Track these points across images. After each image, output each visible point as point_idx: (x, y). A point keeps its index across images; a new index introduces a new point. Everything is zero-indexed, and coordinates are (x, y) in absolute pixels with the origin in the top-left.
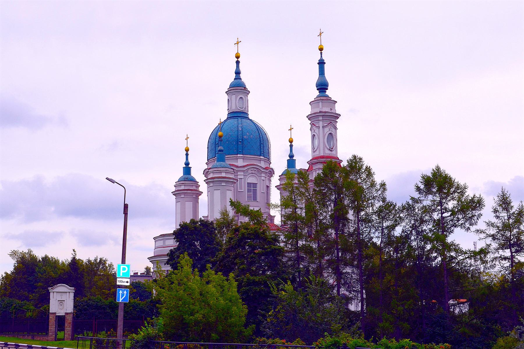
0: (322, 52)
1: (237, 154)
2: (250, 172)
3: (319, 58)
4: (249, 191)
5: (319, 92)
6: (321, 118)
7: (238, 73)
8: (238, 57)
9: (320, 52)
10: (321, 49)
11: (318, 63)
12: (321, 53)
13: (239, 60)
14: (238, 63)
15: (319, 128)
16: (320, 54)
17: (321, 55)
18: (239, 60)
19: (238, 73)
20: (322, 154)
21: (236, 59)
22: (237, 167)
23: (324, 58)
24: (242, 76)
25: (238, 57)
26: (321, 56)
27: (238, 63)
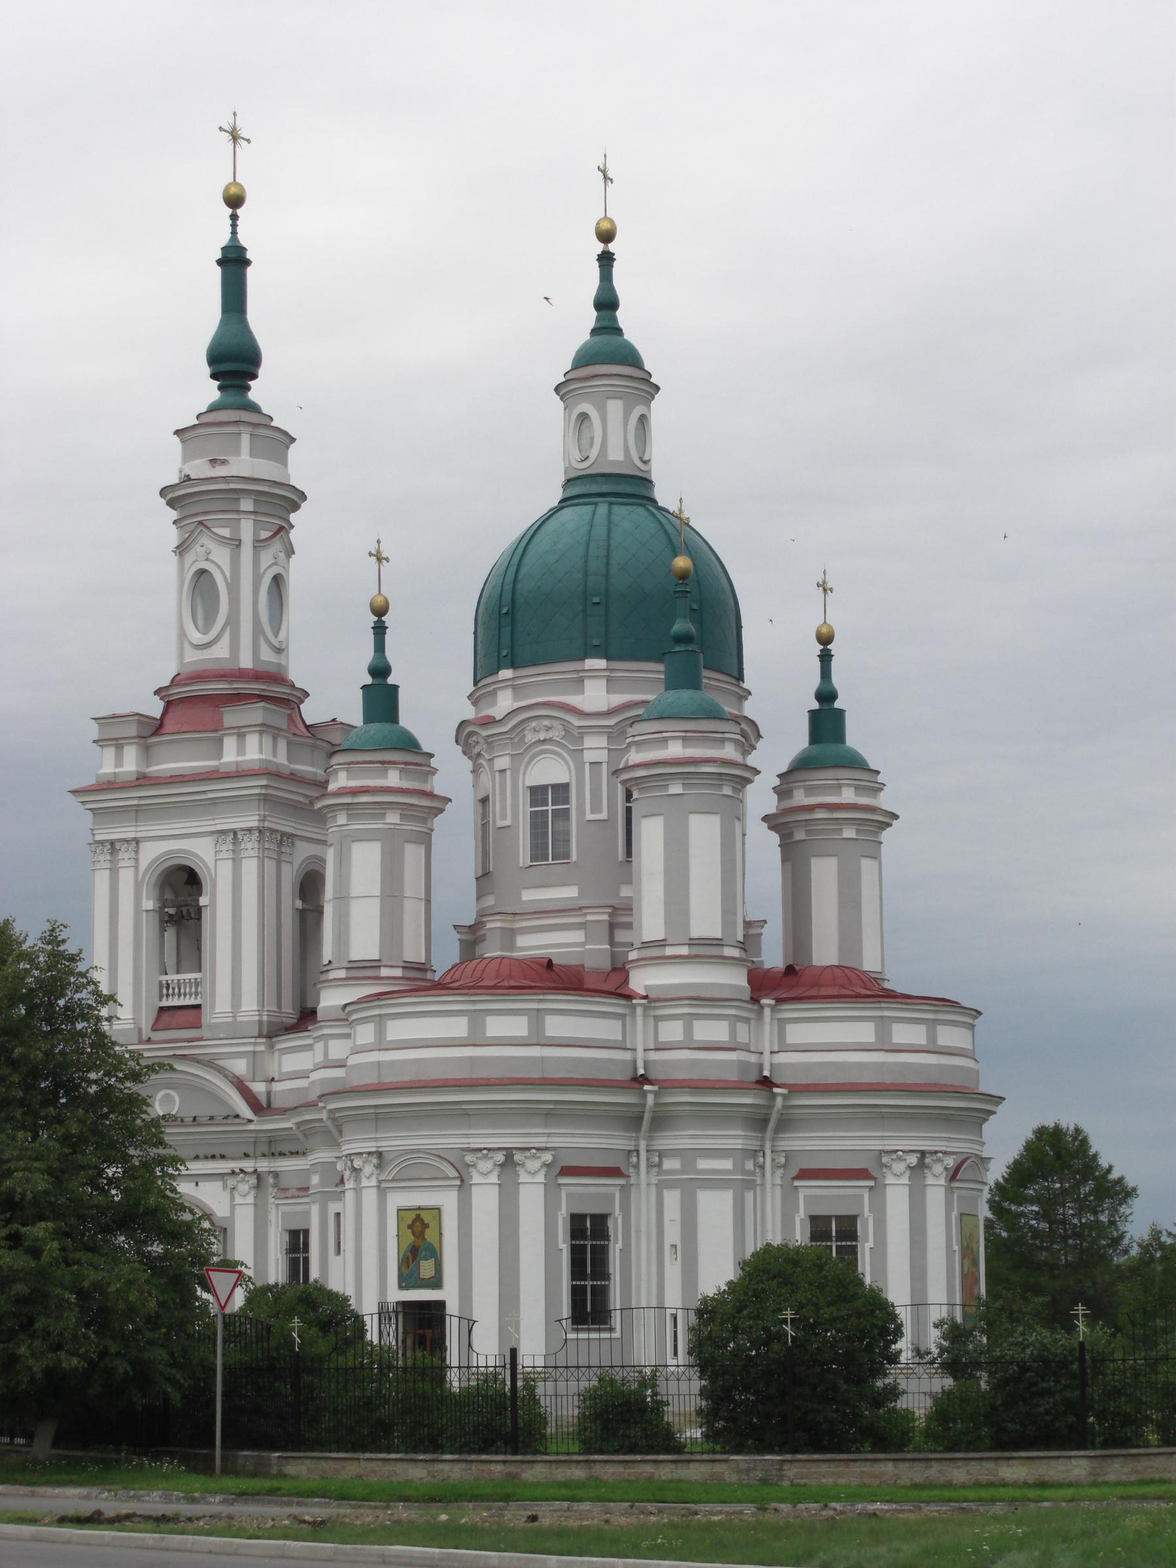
0: (239, 212)
1: (583, 659)
2: (530, 738)
3: (225, 239)
4: (538, 822)
5: (220, 388)
6: (247, 505)
7: (607, 303)
8: (606, 236)
9: (230, 211)
10: (234, 201)
11: (220, 262)
12: (234, 218)
13: (612, 247)
14: (606, 260)
15: (239, 546)
16: (230, 222)
17: (234, 226)
18: (612, 247)
19: (607, 303)
20: (246, 662)
21: (599, 247)
22: (580, 713)
23: (243, 239)
24: (623, 316)
25: (606, 236)
26: (234, 233)
27: (606, 260)
